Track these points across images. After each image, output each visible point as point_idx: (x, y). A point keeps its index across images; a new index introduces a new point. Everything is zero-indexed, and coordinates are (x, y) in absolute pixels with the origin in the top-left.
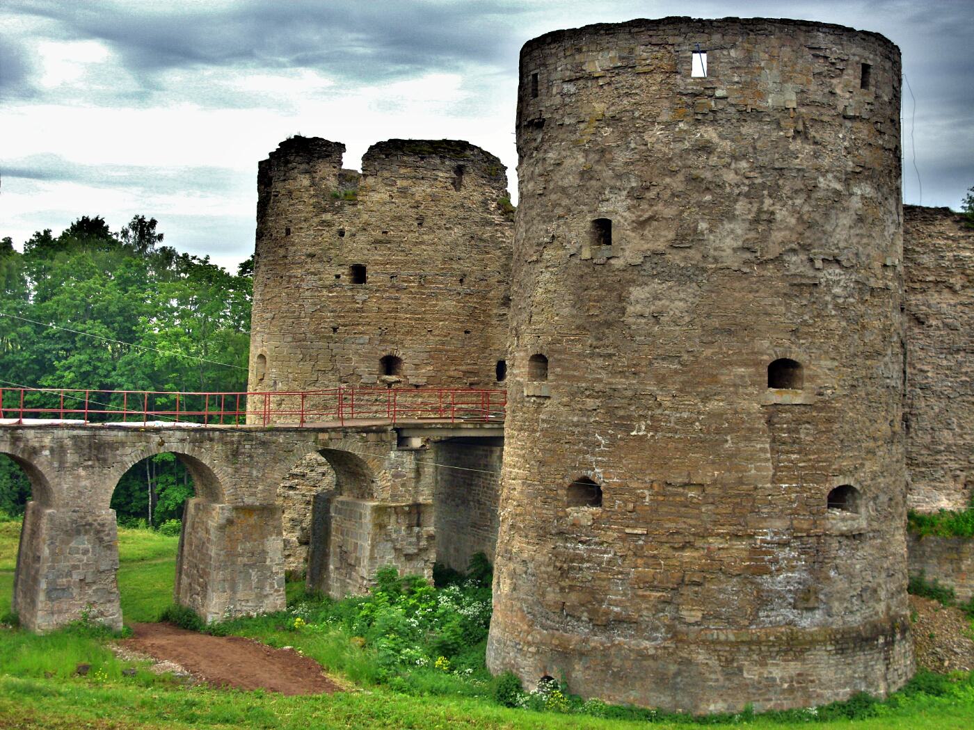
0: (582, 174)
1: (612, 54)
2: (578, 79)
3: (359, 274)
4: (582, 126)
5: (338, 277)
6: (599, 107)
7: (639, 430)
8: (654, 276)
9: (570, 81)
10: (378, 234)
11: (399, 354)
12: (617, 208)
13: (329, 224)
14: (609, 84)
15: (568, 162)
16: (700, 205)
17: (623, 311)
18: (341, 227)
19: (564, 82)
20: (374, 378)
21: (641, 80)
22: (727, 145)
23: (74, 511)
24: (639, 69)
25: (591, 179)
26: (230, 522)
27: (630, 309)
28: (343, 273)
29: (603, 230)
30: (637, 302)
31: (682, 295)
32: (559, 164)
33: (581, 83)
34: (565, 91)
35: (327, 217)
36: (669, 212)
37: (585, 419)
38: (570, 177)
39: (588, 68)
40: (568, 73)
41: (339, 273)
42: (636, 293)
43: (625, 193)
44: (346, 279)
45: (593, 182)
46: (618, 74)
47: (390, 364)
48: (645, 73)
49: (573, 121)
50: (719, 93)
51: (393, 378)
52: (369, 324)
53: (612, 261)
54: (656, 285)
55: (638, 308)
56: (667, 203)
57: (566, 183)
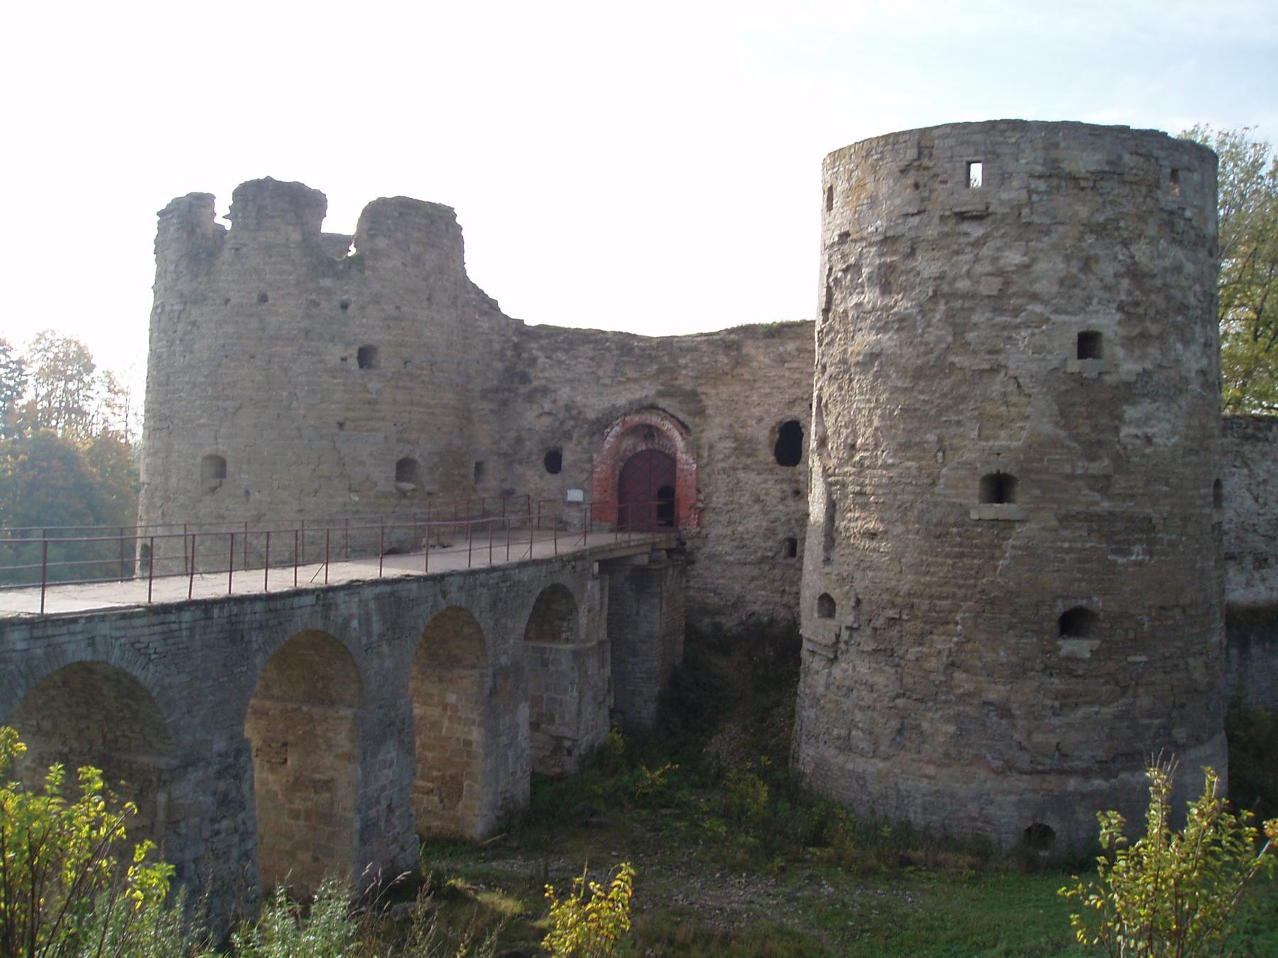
0: (1062, 282)
1: (1098, 156)
2: (1050, 176)
3: (365, 356)
4: (1061, 229)
5: (344, 359)
6: (1083, 212)
7: (1138, 555)
8: (1144, 396)
9: (1040, 177)
10: (390, 309)
11: (416, 456)
12: (1106, 322)
13: (328, 292)
14: (1092, 189)
15: (1041, 266)
16: (1175, 326)
17: (1117, 430)
18: (345, 297)
19: (1032, 176)
20: (390, 487)
21: (1126, 190)
22: (1189, 268)
23: (380, 707)
24: (1127, 178)
25: (1075, 286)
26: (494, 691)
27: (1125, 431)
28: (351, 356)
29: (1088, 344)
30: (1131, 422)
31: (1168, 416)
32: (1028, 266)
33: (1054, 182)
34: (1033, 186)
35: (327, 282)
36: (1154, 329)
37: (1079, 545)
38: (1044, 282)
39: (1067, 167)
40: (1039, 169)
41: (345, 355)
42: (1130, 412)
43: (1115, 305)
44: (353, 363)
45: (1077, 291)
46: (1102, 179)
47: (405, 468)
48: (1131, 183)
49: (1046, 220)
50: (1188, 214)
51: (408, 486)
52: (383, 419)
53: (1106, 378)
54: (1146, 407)
55: (1133, 431)
56: (1154, 321)
57: (1037, 287)
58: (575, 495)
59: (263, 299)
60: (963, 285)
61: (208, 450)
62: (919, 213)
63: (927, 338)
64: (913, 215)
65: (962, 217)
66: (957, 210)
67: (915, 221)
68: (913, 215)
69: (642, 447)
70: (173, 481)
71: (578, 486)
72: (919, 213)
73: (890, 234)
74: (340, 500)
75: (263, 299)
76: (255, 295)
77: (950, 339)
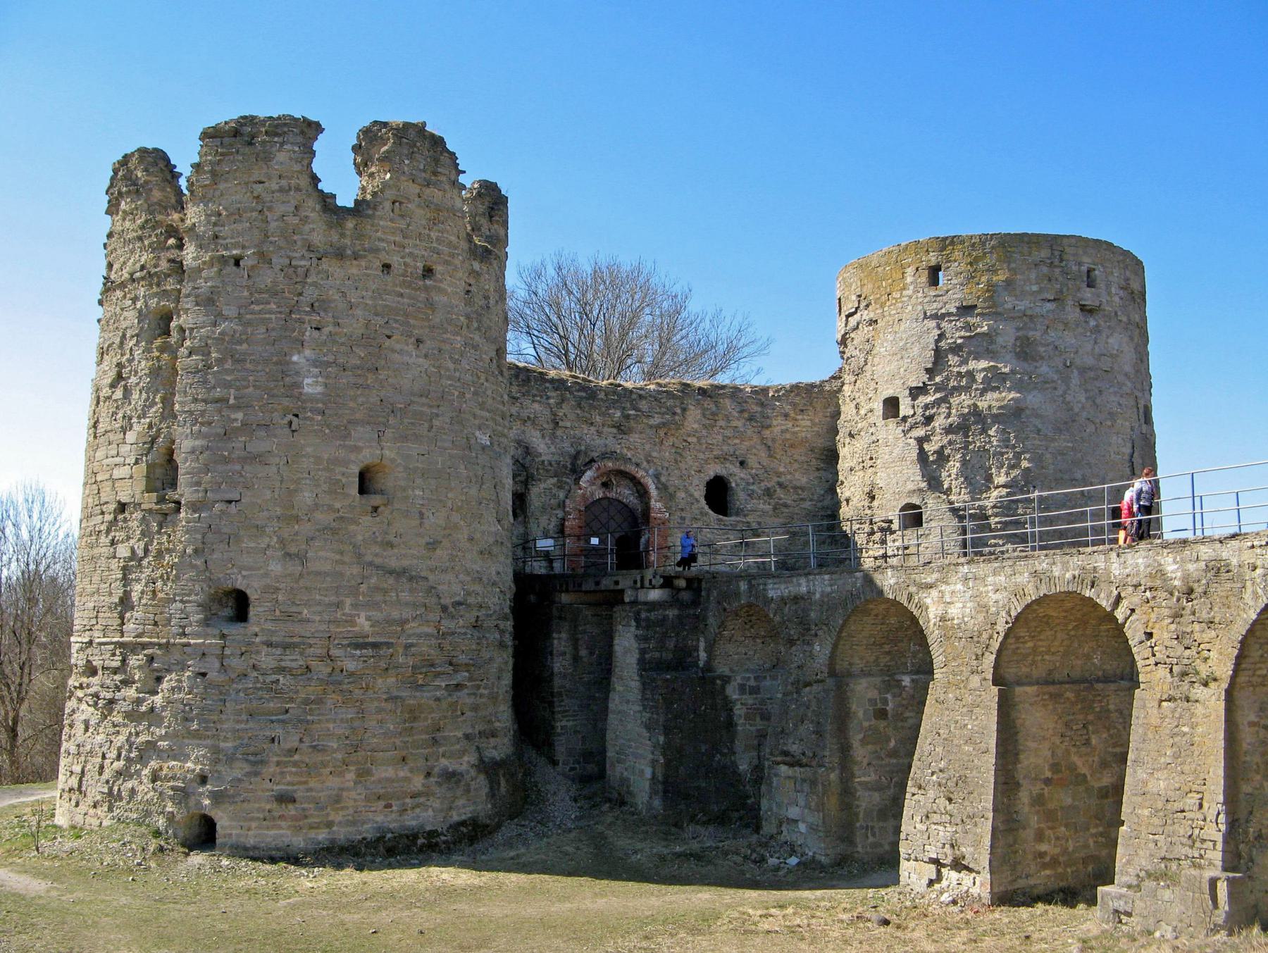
35: (476, 266)
58: (545, 544)
59: (428, 272)
60: (1090, 361)
61: (367, 456)
62: (1055, 300)
63: (1068, 398)
64: (1049, 301)
65: (1083, 308)
66: (1083, 303)
67: (1050, 306)
68: (1049, 301)
69: (599, 494)
70: (306, 497)
71: (546, 536)
72: (1055, 300)
73: (1029, 312)
74: (493, 529)
75: (428, 272)
76: (420, 265)
77: (1083, 400)
